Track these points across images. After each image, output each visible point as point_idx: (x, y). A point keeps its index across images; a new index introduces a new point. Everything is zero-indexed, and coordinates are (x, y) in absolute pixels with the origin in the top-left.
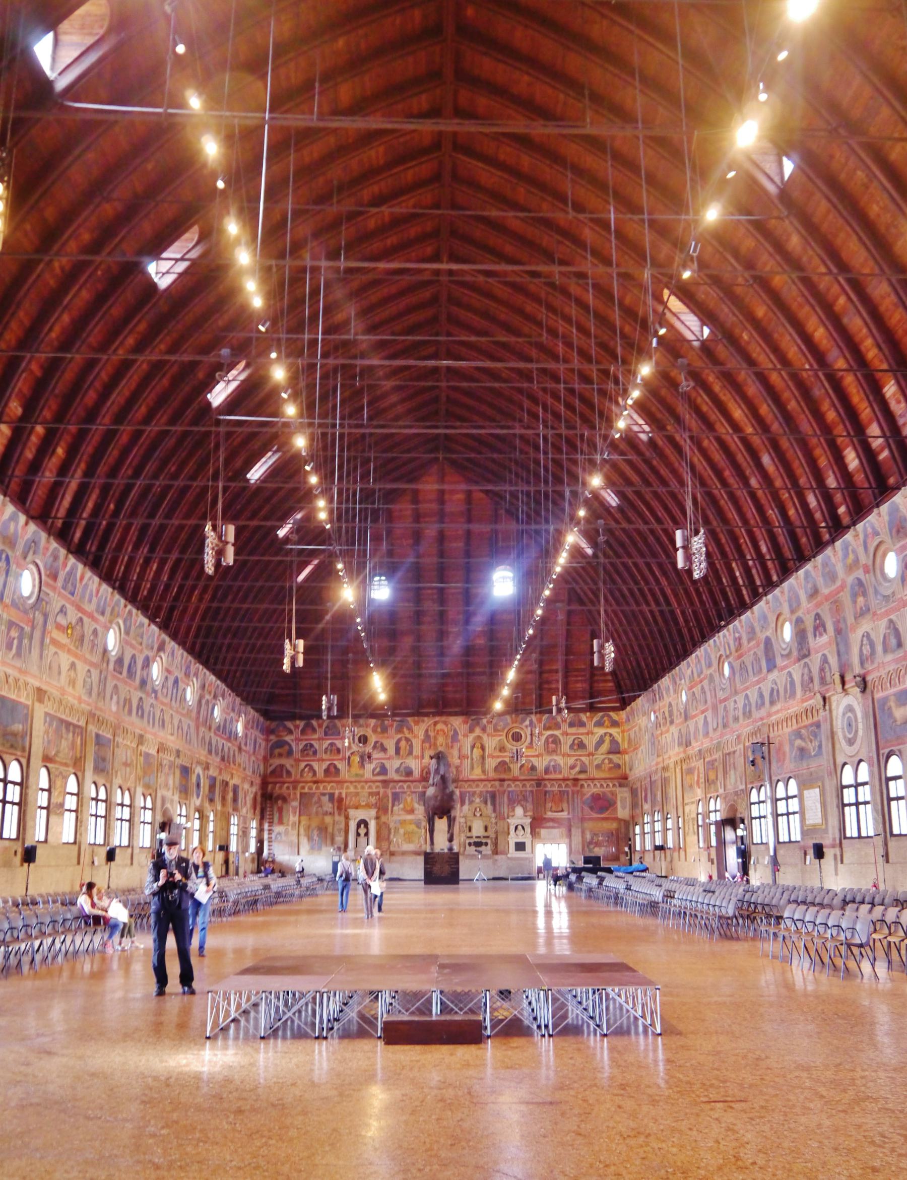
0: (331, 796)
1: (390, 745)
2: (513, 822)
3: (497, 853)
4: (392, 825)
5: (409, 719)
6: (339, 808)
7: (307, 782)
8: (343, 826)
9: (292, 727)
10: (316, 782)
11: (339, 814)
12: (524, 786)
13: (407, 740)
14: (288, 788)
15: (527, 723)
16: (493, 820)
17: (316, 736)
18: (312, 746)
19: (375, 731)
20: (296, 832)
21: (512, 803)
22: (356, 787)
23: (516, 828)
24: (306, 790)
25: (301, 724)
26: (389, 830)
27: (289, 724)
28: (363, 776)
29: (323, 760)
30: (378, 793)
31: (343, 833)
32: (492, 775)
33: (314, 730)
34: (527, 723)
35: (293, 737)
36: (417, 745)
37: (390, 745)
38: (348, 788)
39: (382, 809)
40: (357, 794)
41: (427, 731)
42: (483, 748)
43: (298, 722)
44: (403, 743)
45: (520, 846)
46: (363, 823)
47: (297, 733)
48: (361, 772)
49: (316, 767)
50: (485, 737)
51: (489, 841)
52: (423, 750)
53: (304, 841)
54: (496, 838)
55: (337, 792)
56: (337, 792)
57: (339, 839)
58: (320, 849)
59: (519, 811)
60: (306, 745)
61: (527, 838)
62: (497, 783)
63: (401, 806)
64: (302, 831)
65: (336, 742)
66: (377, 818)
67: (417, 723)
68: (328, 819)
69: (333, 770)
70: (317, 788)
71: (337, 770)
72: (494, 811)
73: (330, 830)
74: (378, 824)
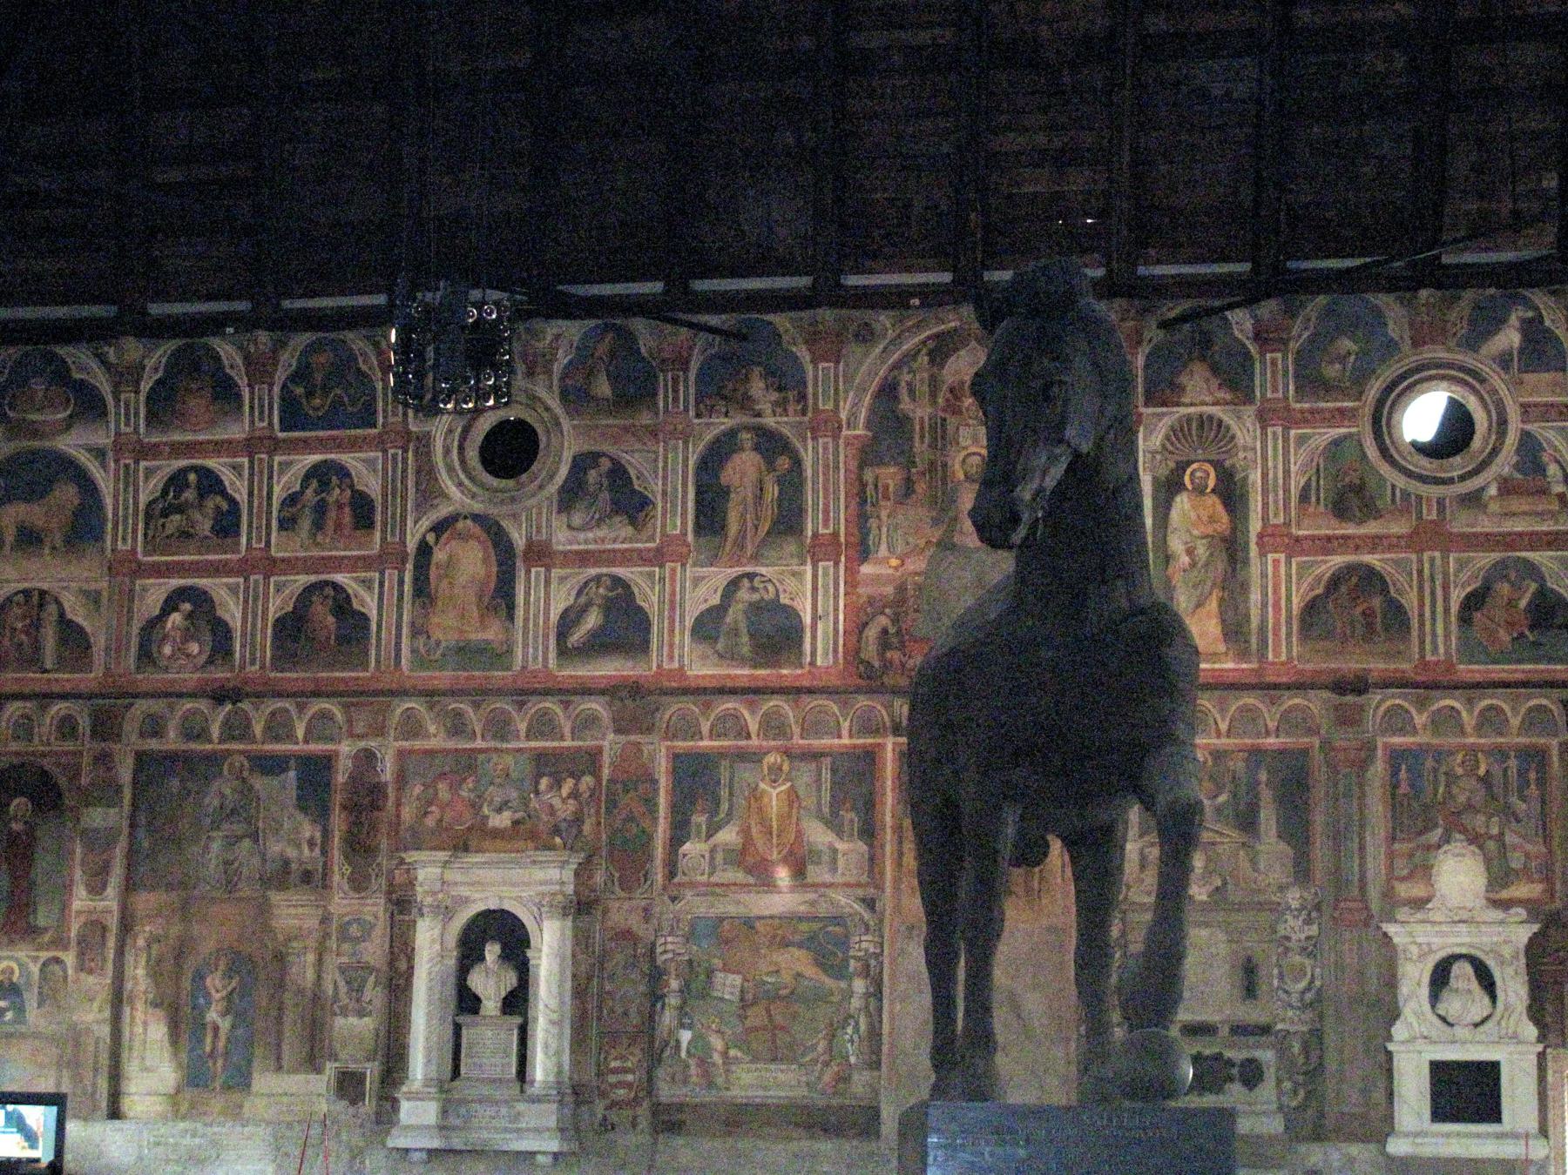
0: (315, 772)
1: (668, 475)
2: (1418, 942)
3: (1318, 1136)
4: (670, 948)
5: (781, 321)
6: (359, 847)
7: (172, 694)
8: (374, 951)
9: (102, 383)
10: (220, 696)
11: (359, 883)
12: (1491, 720)
13: (771, 445)
14: (67, 727)
15: (1510, 338)
16: (1295, 928)
17: (236, 431)
18: (210, 483)
19: (576, 397)
20: (98, 984)
21: (1423, 815)
22: (458, 727)
23: (1440, 977)
24: (172, 741)
25: (155, 358)
26: (656, 976)
27: (81, 360)
28: (499, 656)
29: (272, 566)
30: (593, 758)
31: (374, 994)
32: (1285, 651)
33: (225, 393)
34: (1510, 338)
35: (103, 438)
36: (826, 469)
37: (668, 475)
38: (412, 727)
39: (615, 856)
40: (467, 764)
41: (888, 391)
42: (1231, 492)
43: (132, 349)
44: (743, 468)
45: (1467, 1092)
46: (500, 933)
47: (128, 415)
48: (492, 633)
49: (232, 611)
50: (1244, 428)
51: (1267, 1056)
52: (862, 500)
53: (149, 1034)
54: (1317, 1034)
55: (346, 749)
56: (346, 749)
57: (355, 1029)
58: (240, 1081)
59: (1459, 875)
60: (177, 481)
61: (1513, 1051)
62: (1317, 704)
63: (728, 836)
64: (138, 975)
65: (346, 459)
66: (581, 907)
67: (828, 346)
68: (292, 913)
69: (324, 618)
70: (237, 729)
71: (352, 624)
72: (1302, 871)
73: (303, 970)
74: (581, 940)
